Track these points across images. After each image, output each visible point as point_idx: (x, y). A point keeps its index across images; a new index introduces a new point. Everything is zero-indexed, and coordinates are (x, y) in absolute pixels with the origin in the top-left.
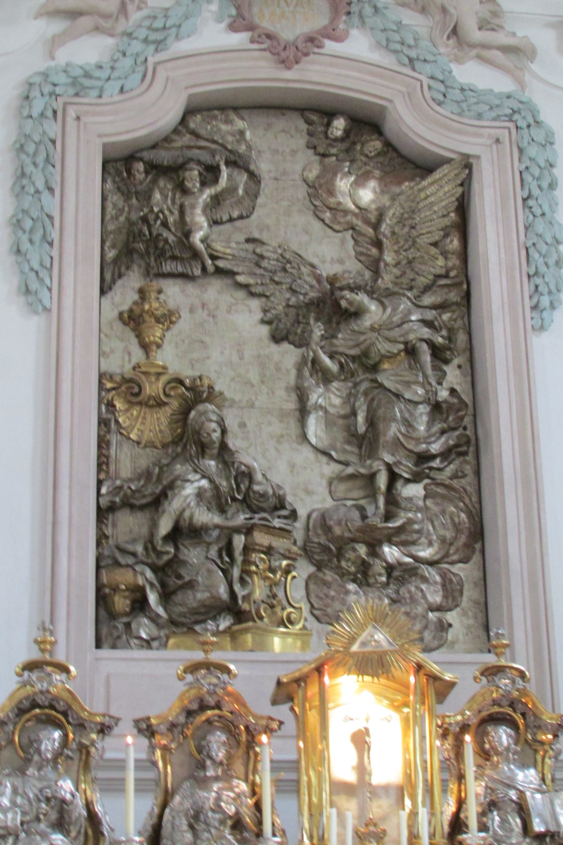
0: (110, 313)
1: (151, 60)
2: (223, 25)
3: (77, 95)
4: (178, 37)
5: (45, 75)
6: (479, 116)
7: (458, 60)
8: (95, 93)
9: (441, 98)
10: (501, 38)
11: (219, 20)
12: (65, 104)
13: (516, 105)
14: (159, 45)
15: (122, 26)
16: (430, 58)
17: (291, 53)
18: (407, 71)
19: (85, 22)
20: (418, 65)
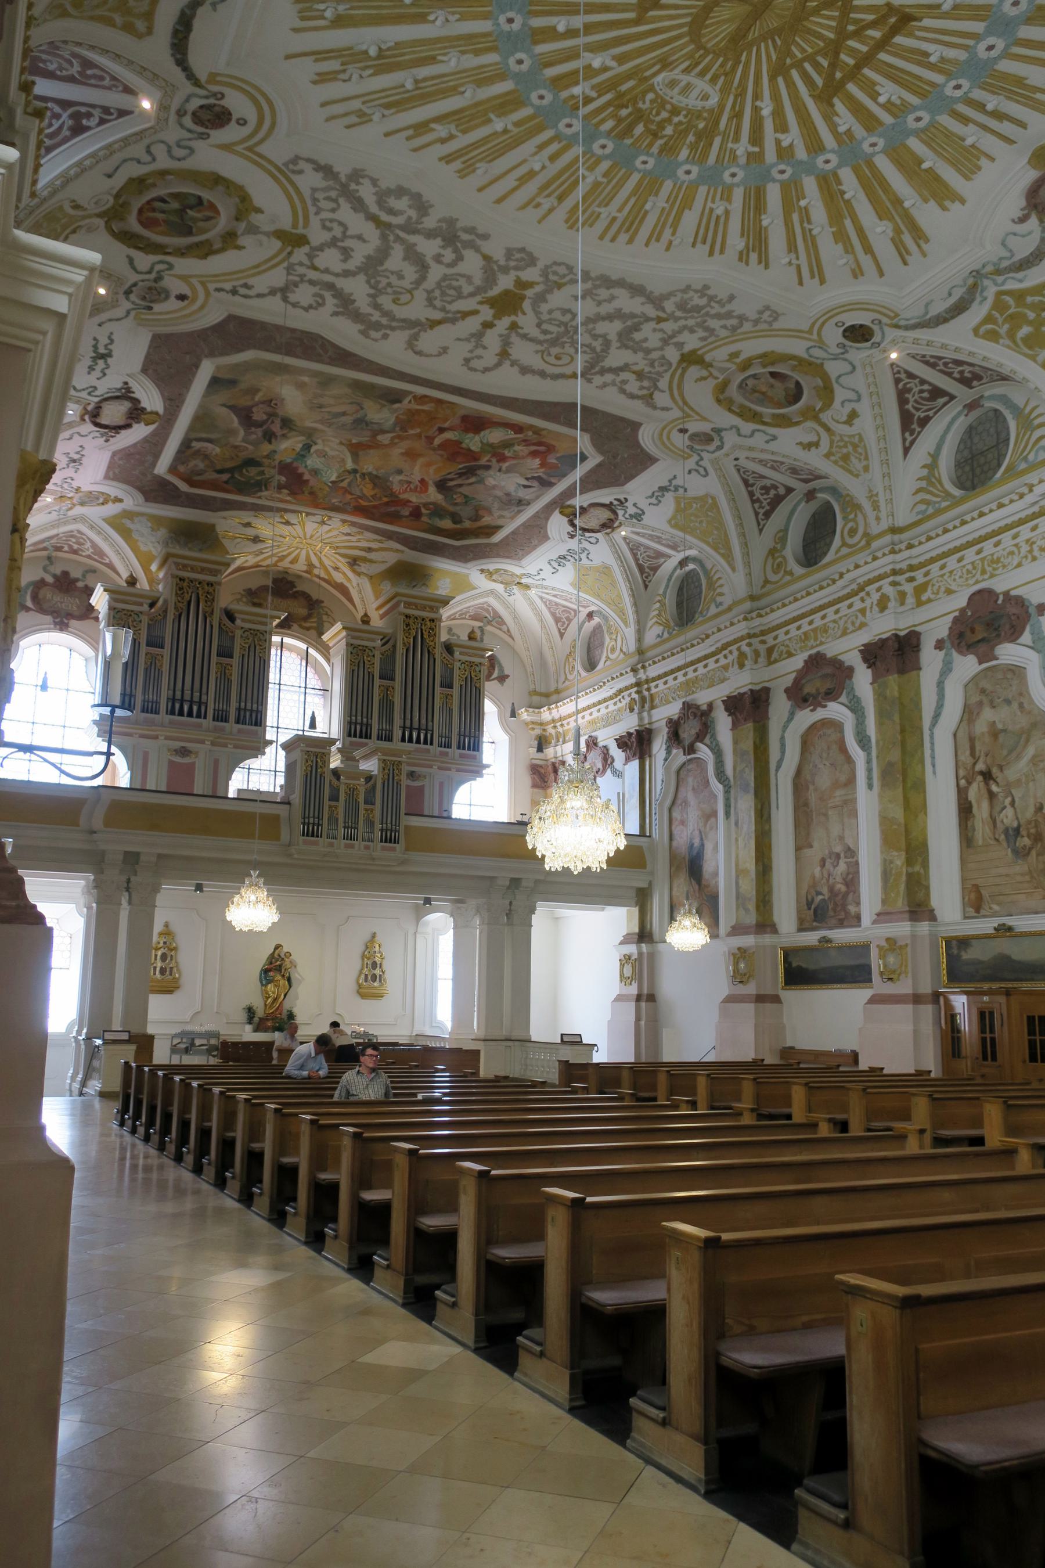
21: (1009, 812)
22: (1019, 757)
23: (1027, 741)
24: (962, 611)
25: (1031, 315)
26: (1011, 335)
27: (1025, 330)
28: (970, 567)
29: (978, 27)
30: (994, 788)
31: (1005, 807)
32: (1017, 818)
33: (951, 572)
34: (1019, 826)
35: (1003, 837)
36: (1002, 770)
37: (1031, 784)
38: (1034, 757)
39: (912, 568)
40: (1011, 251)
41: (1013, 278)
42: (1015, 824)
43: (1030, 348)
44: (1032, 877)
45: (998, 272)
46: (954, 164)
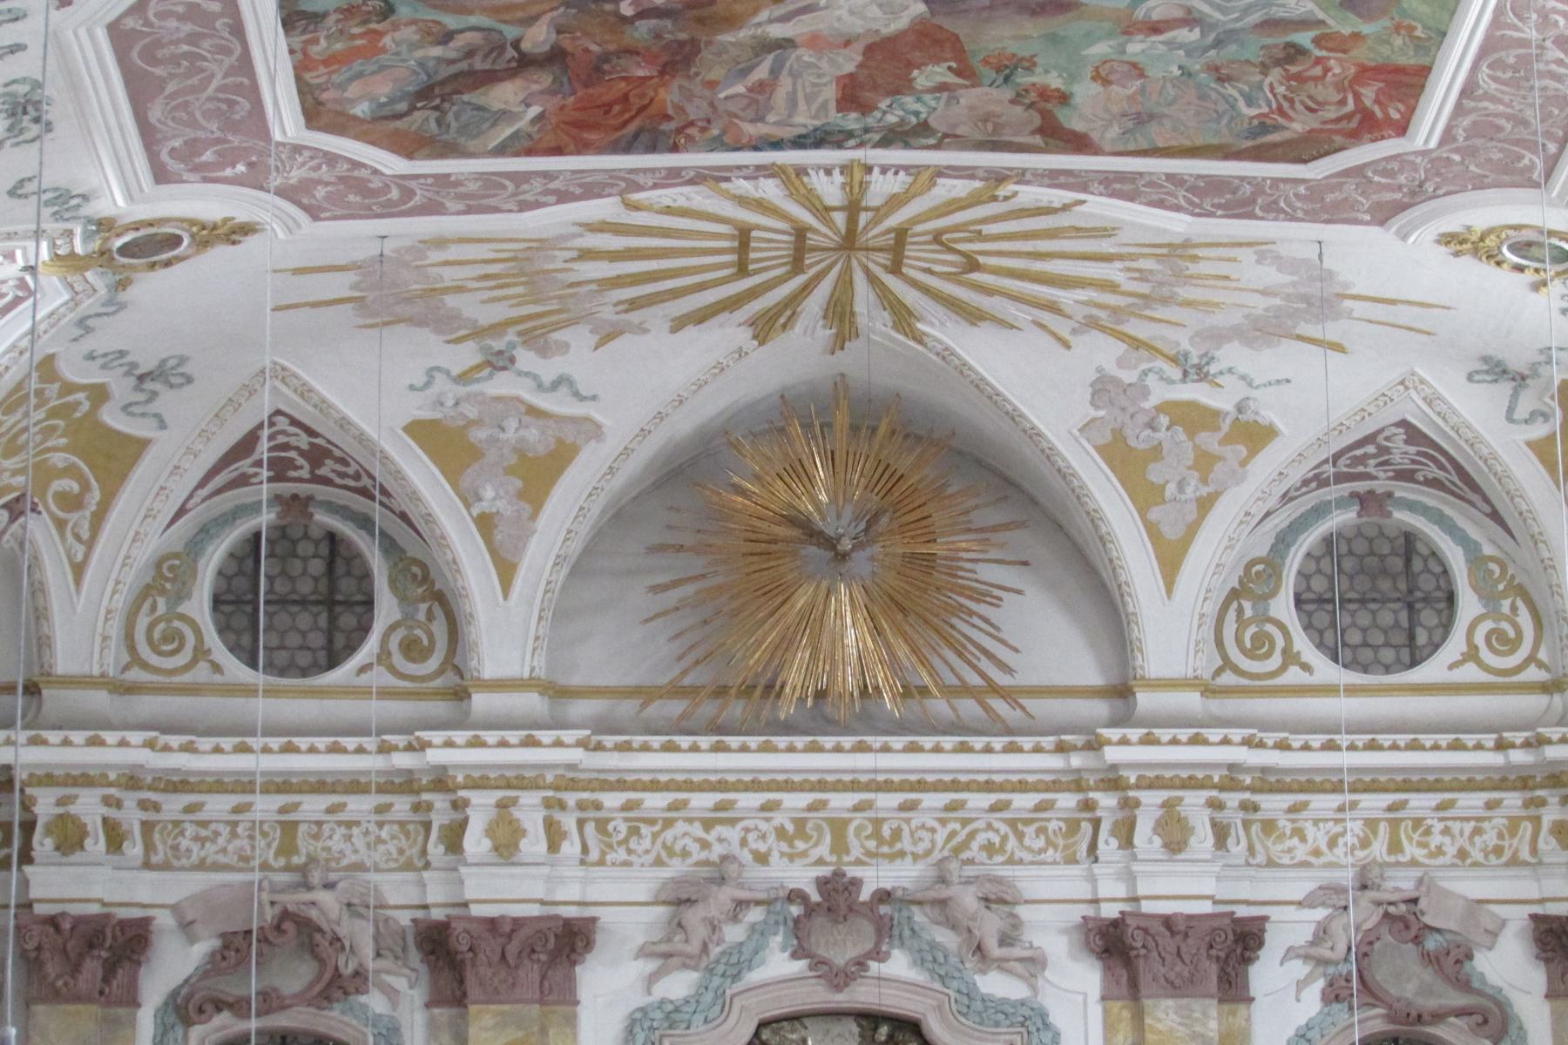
1: (729, 993)
2: (787, 954)
3: (670, 1027)
4: (750, 969)
5: (643, 1010)
6: (997, 1024)
7: (983, 972)
8: (684, 1025)
9: (965, 1010)
10: (1017, 952)
11: (783, 949)
12: (662, 1037)
13: (1028, 1013)
14: (736, 977)
15: (704, 962)
16: (956, 974)
17: (841, 979)
18: (937, 986)
19: (675, 961)
20: (948, 981)
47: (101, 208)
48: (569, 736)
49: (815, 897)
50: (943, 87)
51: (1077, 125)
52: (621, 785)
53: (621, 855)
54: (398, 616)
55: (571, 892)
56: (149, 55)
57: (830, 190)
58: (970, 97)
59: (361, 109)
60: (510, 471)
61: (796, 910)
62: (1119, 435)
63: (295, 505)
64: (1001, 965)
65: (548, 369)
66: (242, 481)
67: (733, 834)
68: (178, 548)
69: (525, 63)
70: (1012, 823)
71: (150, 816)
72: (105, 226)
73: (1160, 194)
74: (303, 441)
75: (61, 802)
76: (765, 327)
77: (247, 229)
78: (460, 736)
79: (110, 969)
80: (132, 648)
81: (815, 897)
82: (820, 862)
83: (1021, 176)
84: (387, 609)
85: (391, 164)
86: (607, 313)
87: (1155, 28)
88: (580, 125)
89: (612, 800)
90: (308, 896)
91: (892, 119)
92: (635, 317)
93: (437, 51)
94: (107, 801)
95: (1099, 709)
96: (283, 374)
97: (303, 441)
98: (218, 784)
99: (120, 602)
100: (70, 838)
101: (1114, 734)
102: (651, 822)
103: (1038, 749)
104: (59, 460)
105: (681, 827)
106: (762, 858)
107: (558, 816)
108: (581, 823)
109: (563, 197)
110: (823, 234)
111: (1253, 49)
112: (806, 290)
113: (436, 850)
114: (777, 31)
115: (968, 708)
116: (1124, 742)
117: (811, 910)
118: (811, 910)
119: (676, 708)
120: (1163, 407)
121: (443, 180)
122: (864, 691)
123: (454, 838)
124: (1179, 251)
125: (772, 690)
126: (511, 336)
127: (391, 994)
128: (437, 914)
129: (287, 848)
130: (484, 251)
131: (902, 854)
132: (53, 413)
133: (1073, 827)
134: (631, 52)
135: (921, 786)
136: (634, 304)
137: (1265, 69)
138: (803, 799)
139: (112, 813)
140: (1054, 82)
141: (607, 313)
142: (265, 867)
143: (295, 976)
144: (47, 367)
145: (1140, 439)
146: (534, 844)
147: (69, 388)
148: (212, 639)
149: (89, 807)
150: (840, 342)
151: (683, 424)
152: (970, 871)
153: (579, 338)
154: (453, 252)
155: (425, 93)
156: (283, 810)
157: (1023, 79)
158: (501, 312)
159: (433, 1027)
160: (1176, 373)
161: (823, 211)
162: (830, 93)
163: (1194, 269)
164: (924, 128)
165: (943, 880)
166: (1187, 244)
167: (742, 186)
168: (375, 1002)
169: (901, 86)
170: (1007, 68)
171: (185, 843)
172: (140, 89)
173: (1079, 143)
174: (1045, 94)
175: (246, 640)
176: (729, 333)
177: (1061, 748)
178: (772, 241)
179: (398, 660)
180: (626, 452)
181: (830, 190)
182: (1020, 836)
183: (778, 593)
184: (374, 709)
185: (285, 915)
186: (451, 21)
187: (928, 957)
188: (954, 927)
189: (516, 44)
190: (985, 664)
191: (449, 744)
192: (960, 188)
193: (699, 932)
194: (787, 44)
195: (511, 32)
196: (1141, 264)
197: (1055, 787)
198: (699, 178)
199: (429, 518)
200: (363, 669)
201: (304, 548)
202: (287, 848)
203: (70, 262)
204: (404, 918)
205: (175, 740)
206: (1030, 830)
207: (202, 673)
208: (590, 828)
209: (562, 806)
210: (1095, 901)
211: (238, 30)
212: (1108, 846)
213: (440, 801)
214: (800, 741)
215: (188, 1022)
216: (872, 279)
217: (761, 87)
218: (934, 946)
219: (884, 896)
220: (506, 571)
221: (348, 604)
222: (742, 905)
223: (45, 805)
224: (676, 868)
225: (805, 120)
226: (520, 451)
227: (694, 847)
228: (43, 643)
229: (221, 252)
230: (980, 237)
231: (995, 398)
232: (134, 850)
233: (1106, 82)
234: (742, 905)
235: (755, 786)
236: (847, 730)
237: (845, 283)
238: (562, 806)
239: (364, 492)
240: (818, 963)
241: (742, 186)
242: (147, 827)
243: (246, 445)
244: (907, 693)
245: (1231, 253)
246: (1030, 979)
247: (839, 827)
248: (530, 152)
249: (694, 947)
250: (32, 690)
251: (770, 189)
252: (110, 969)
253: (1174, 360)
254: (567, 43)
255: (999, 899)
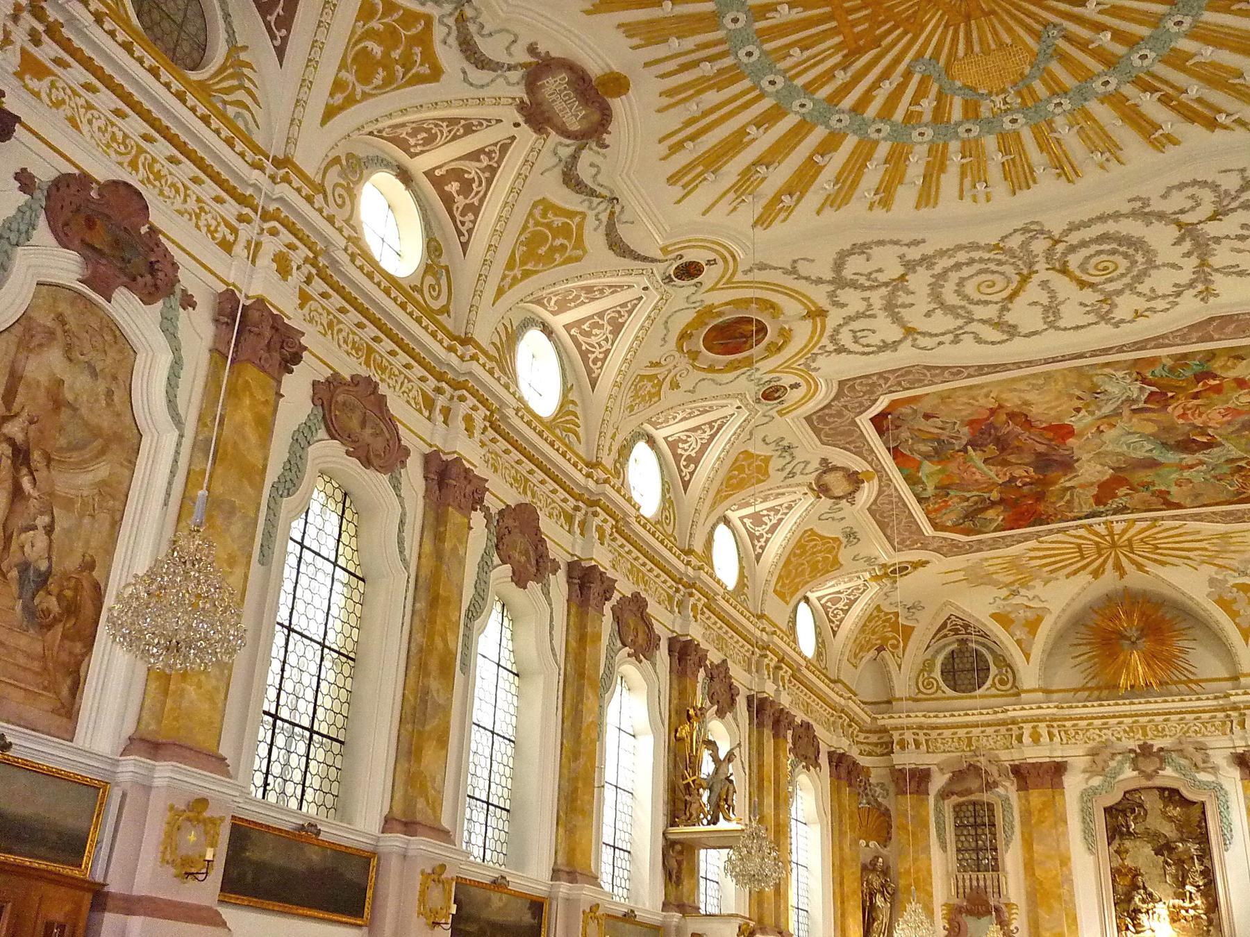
0: (1112, 851)
10: (1209, 765)
14: (1114, 778)
21: (41, 540)
22: (81, 466)
23: (102, 452)
24: (84, 180)
25: (396, 55)
26: (370, 34)
27: (377, 50)
28: (120, 136)
29: (799, 82)
30: (26, 483)
31: (34, 528)
32: (49, 558)
33: (89, 107)
34: (49, 572)
35: (14, 573)
36: (48, 466)
37: (86, 520)
38: (103, 484)
39: (53, 31)
40: (490, 35)
41: (449, 34)
42: (43, 566)
43: (354, 59)
44: (45, 669)
45: (461, 20)
46: (650, 22)
47: (881, 561)
48: (1051, 705)
49: (1138, 751)
50: (1127, 494)
51: (1176, 501)
52: (1071, 719)
53: (1073, 740)
54: (997, 672)
55: (1059, 753)
56: (881, 516)
57: (1102, 530)
58: (1136, 496)
59: (949, 524)
60: (1024, 626)
61: (1132, 755)
62: (1220, 596)
63: (963, 642)
64: (1204, 770)
65: (1030, 594)
66: (946, 636)
67: (1109, 732)
68: (929, 657)
69: (993, 504)
70: (1202, 723)
71: (927, 737)
72: (884, 566)
73: (1212, 518)
74: (961, 622)
75: (900, 735)
76: (1096, 574)
77: (927, 562)
78: (1017, 707)
79: (919, 785)
80: (919, 689)
81: (1138, 751)
82: (1139, 739)
83: (1163, 519)
84: (993, 670)
85: (964, 538)
86: (1045, 575)
87: (1191, 467)
88: (1016, 520)
89: (1069, 724)
90: (975, 759)
91: (1114, 506)
92: (1054, 575)
93: (966, 504)
94: (914, 734)
95: (1229, 684)
96: (951, 604)
97: (961, 622)
98: (947, 727)
99: (914, 674)
100: (903, 745)
101: (1233, 692)
102: (1082, 730)
103: (1208, 699)
104: (890, 635)
105: (1092, 731)
106: (1119, 739)
107: (1051, 729)
108: (1059, 732)
109: (1019, 542)
110: (1105, 544)
111: (1226, 469)
112: (1105, 562)
113: (1015, 742)
114: (1068, 484)
115: (1182, 687)
116: (1237, 694)
117: (1137, 755)
118: (1137, 755)
119: (1086, 693)
120: (1234, 586)
121: (980, 541)
122: (1146, 684)
123: (1020, 739)
124: (1224, 536)
125: (1117, 687)
126: (1017, 585)
127: (1006, 788)
128: (1017, 763)
129: (970, 744)
130: (1000, 561)
131: (1166, 735)
132: (884, 621)
133: (1224, 723)
134: (1025, 496)
135: (1170, 713)
136: (1052, 572)
137: (1232, 475)
138: (1129, 720)
139: (916, 737)
140: (1163, 488)
141: (1045, 575)
142: (963, 751)
143: (974, 784)
144: (878, 608)
145: (1228, 596)
146: (1045, 738)
147: (887, 614)
148: (942, 683)
149: (909, 736)
150: (1122, 577)
151: (1077, 606)
152: (1189, 740)
153: (1038, 583)
154: (990, 562)
155: (966, 517)
156: (967, 733)
157: (1152, 488)
158: (1011, 579)
159: (1019, 797)
160: (1236, 574)
161: (1102, 537)
162: (1092, 501)
163: (1234, 540)
164: (1125, 508)
165: (1180, 743)
166: (1226, 533)
167: (1072, 532)
168: (1001, 790)
169: (1115, 496)
170: (1146, 486)
171: (938, 745)
172: (882, 526)
173: (1179, 506)
174: (1161, 492)
175: (952, 683)
176: (1084, 578)
177: (1216, 698)
178: (1090, 550)
179: (998, 685)
180: (1059, 617)
181: (1102, 530)
182: (1206, 728)
183: (1113, 655)
184: (992, 701)
185: (970, 765)
186: (968, 495)
187: (1178, 768)
188: (1186, 758)
189: (989, 499)
190: (1186, 673)
191: (1014, 710)
192: (1144, 524)
193: (1101, 764)
194: (1072, 487)
195: (986, 495)
196: (1215, 541)
197: (1216, 710)
198: (1059, 531)
199: (1001, 641)
200: (988, 689)
201: (967, 654)
202: (970, 744)
203: (876, 578)
204: (1007, 764)
205: (932, 714)
206: (1209, 725)
207: (939, 694)
208: (1062, 733)
209: (1053, 727)
210: (1234, 747)
211: (905, 505)
212: (1237, 728)
213: (1014, 727)
214: (1127, 701)
215: (943, 799)
216: (1125, 555)
217: (1068, 502)
218: (1180, 764)
219: (1161, 749)
220: (1027, 656)
221: (983, 669)
222: (1114, 754)
223: (896, 736)
224: (1091, 744)
225: (1086, 510)
226: (1026, 619)
227: (1097, 737)
228: (892, 688)
229: (921, 569)
230: (1156, 539)
231: (1175, 588)
232: (923, 748)
233: (1180, 486)
234: (1114, 754)
235: (1114, 717)
236: (1142, 696)
237: (1117, 557)
238: (1053, 727)
239: (982, 636)
240: (1141, 772)
241: (1072, 532)
242: (927, 741)
243: (944, 625)
244: (1161, 684)
245: (1243, 534)
246: (1215, 774)
247: (1144, 728)
248: (1004, 530)
249: (1100, 769)
250: (889, 702)
251: (1082, 532)
252: (919, 785)
253: (1234, 571)
254: (1004, 496)
255: (1201, 748)
